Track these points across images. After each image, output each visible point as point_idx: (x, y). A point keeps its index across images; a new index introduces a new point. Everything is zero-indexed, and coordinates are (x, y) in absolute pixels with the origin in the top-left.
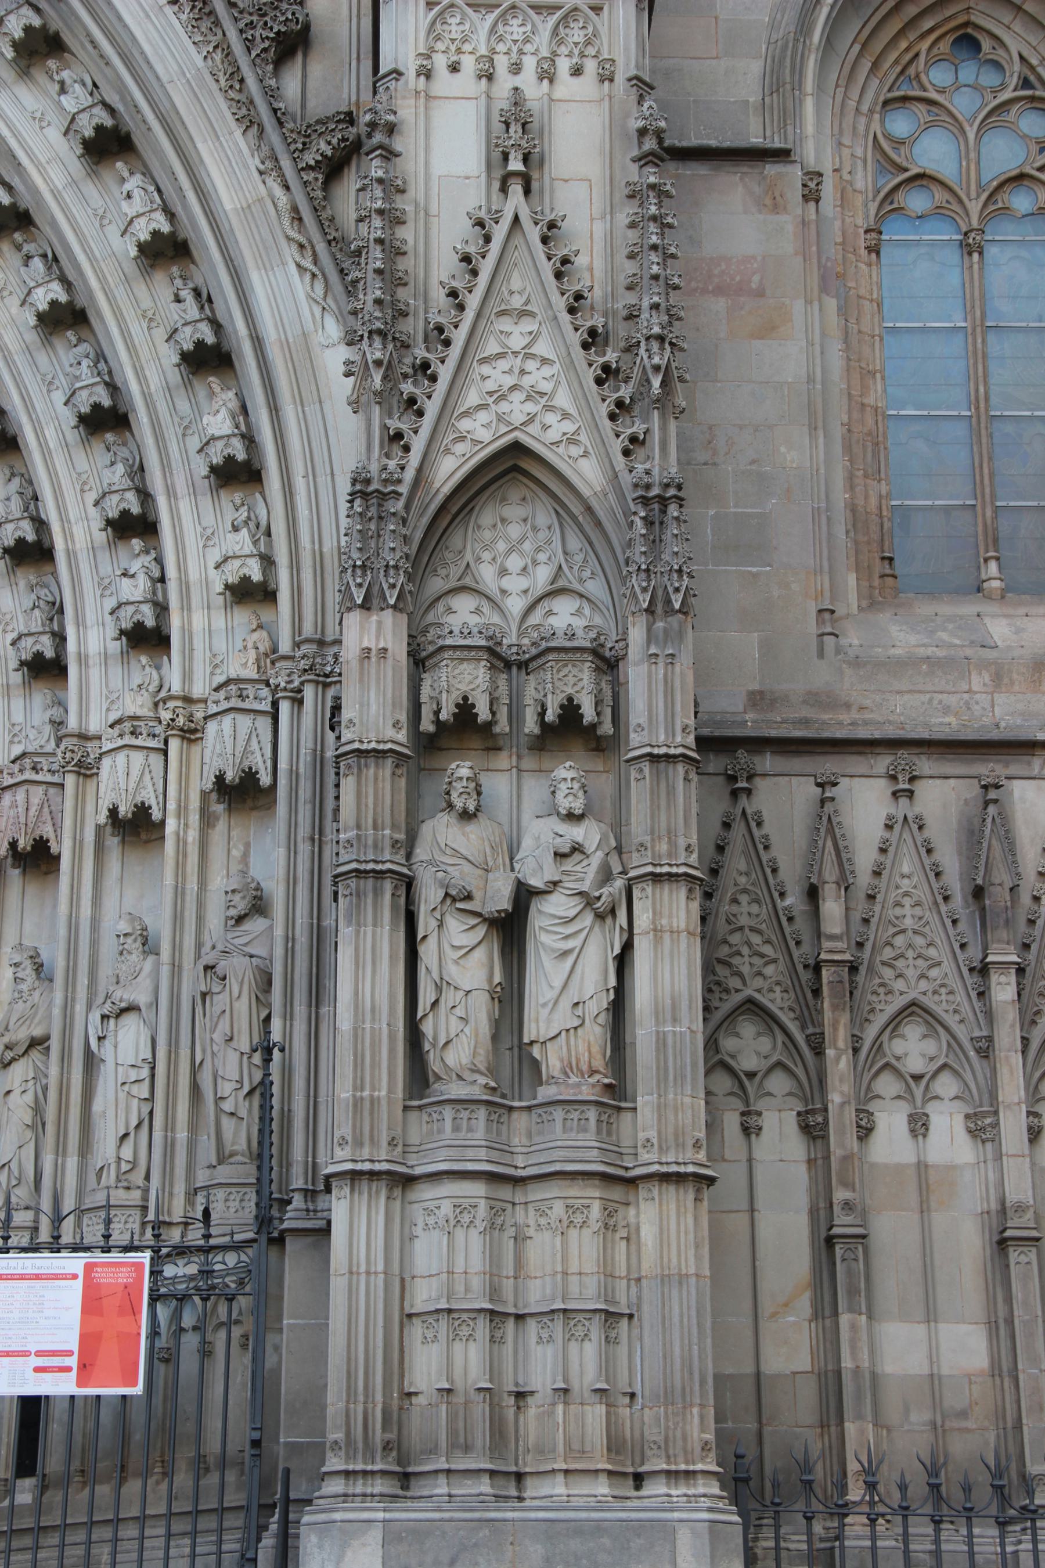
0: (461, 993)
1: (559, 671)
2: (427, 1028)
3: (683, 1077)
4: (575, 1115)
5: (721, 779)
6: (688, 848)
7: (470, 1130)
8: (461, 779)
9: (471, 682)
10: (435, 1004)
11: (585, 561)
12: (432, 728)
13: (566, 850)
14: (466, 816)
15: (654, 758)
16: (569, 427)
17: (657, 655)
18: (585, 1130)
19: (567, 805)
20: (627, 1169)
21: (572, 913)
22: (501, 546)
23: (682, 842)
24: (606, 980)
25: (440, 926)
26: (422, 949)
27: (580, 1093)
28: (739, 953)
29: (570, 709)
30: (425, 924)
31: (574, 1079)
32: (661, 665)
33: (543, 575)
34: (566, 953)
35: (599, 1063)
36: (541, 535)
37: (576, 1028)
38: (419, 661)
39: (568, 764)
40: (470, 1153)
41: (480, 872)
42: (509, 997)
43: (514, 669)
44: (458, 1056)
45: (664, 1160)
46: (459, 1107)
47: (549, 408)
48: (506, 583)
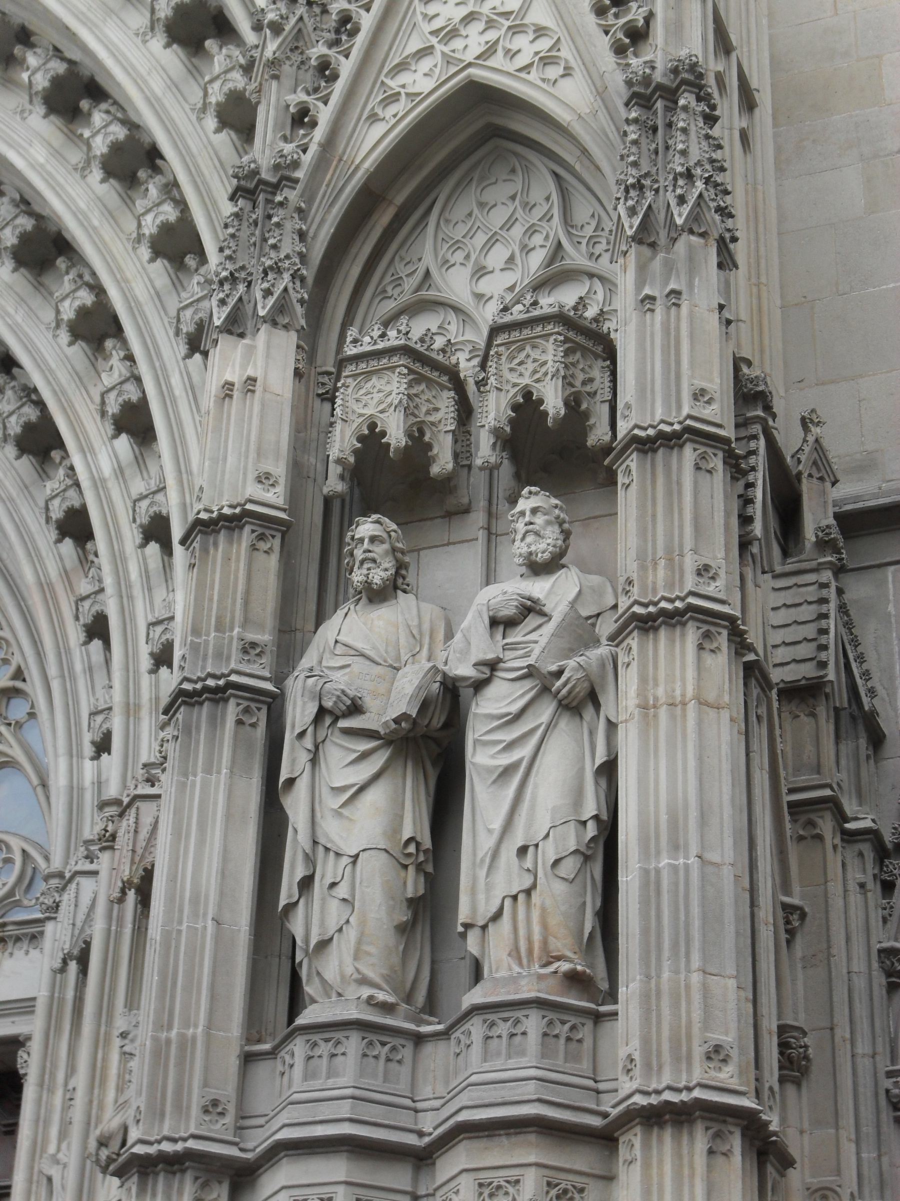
0: (345, 860)
1: (511, 358)
6: (703, 571)
8: (361, 540)
10: (306, 883)
13: (509, 611)
14: (377, 595)
16: (544, 44)
17: (652, 299)
18: (522, 1053)
22: (481, 239)
23: (690, 563)
25: (314, 761)
29: (527, 406)
33: (537, 259)
34: (507, 771)
35: (562, 944)
36: (538, 213)
37: (528, 892)
46: (315, 1037)
47: (516, 30)
48: (484, 286)
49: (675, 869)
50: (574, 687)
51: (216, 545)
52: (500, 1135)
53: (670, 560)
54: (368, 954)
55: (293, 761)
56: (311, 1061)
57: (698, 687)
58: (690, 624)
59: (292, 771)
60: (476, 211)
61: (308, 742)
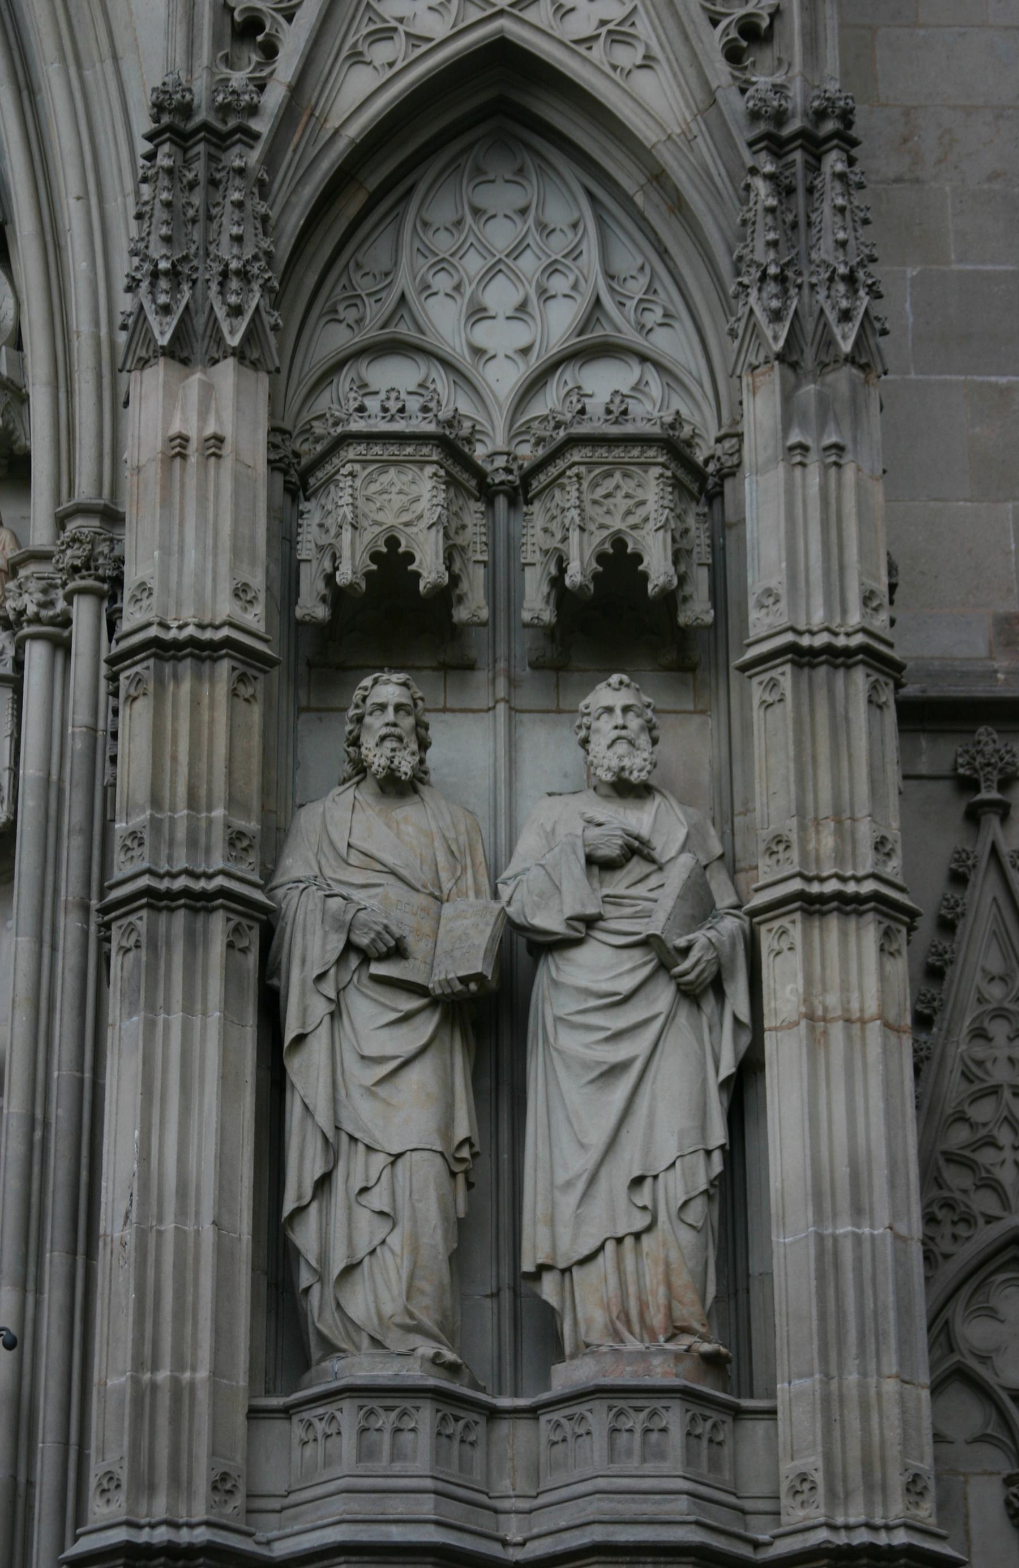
0: (380, 1160)
1: (595, 485)
2: (306, 1238)
3: (879, 1336)
4: (637, 1421)
5: (944, 788)
7: (396, 1455)
8: (382, 707)
9: (404, 510)
10: (324, 1183)
11: (650, 289)
12: (321, 612)
13: (611, 850)
14: (398, 787)
15: (801, 657)
17: (804, 448)
19: (615, 763)
20: (757, 1545)
21: (626, 985)
22: (474, 264)
23: (865, 832)
24: (703, 1128)
25: (335, 1016)
26: (295, 1066)
27: (648, 1372)
28: (991, 1142)
29: (619, 562)
30: (303, 1008)
31: (633, 1344)
34: (614, 1071)
35: (690, 1312)
36: (559, 244)
37: (637, 1236)
38: (296, 475)
39: (615, 678)
40: (397, 1507)
42: (488, 1168)
43: (501, 502)
44: (377, 1296)
45: (840, 1520)
46: (374, 1404)
48: (483, 335)
49: (858, 1239)
50: (702, 971)
51: (176, 677)
52: (645, 1563)
53: (839, 822)
54: (423, 1292)
55: (304, 1011)
56: (366, 1434)
57: (883, 1004)
58: (870, 916)
59: (304, 1025)
60: (469, 219)
61: (329, 988)
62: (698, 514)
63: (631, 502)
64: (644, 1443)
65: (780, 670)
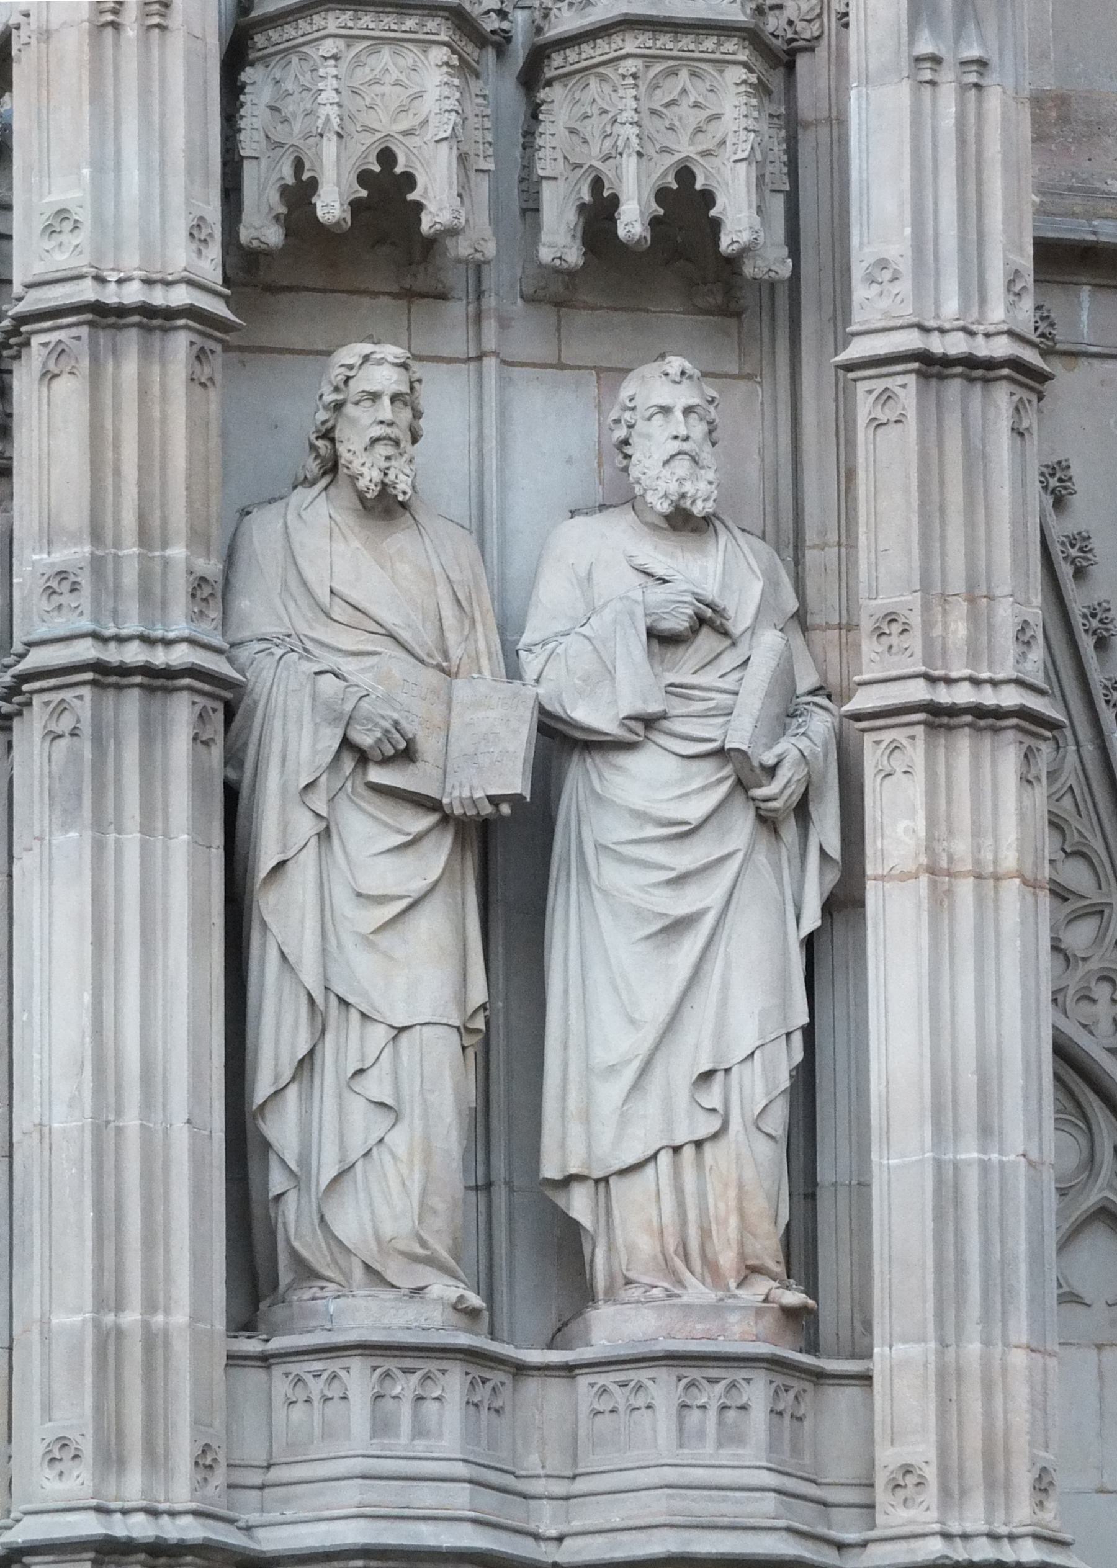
0: (379, 1034)
2: (282, 1130)
3: (1008, 1293)
4: (711, 1396)
8: (374, 396)
9: (403, 110)
13: (678, 623)
15: (931, 367)
17: (936, 60)
19: (673, 488)
21: (695, 810)
24: (785, 1005)
25: (325, 835)
26: (269, 905)
27: (723, 1331)
29: (686, 205)
31: (697, 1291)
32: (948, 93)
34: (678, 926)
37: (699, 1144)
39: (675, 364)
40: (425, 1497)
41: (432, 677)
42: (507, 1047)
45: (955, 1528)
46: (391, 1364)
49: (985, 1167)
51: (115, 352)
53: (972, 600)
54: (435, 1212)
55: (285, 827)
56: (382, 1403)
58: (1010, 735)
62: (771, 115)
63: (703, 115)
64: (720, 1423)
65: (900, 380)
